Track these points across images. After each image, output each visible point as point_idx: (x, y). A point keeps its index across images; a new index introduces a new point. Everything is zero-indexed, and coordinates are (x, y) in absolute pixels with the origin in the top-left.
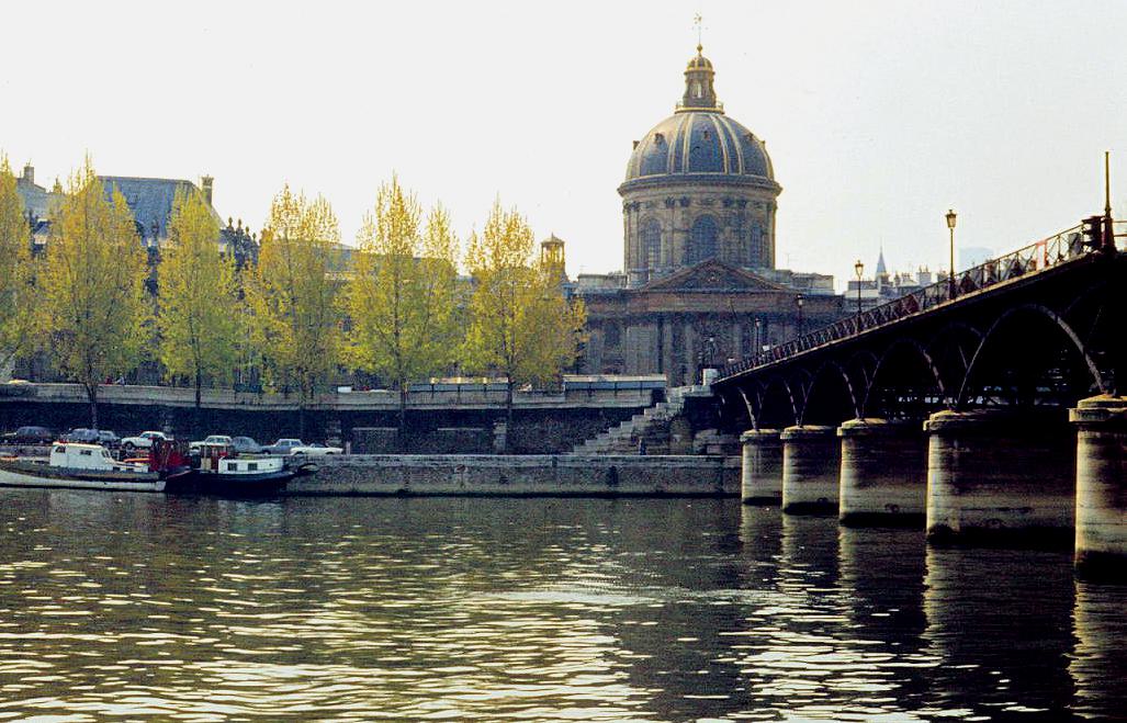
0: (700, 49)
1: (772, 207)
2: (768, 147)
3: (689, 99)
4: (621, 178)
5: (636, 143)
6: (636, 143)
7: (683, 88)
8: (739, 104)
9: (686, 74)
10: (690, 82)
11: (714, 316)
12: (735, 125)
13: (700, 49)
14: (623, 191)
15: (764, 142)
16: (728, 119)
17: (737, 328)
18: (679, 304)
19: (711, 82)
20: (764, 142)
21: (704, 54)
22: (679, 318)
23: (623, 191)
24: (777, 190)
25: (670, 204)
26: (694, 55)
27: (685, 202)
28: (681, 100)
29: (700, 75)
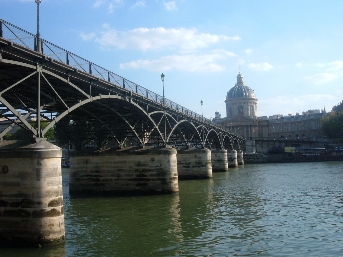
4: (225, 99)
5: (228, 92)
6: (228, 92)
7: (237, 80)
9: (237, 78)
10: (238, 79)
11: (240, 126)
13: (239, 72)
14: (225, 102)
15: (253, 90)
16: (245, 86)
17: (245, 128)
19: (242, 79)
20: (253, 90)
21: (240, 74)
22: (233, 127)
23: (225, 102)
25: (233, 104)
26: (239, 74)
27: (236, 104)
28: (236, 82)
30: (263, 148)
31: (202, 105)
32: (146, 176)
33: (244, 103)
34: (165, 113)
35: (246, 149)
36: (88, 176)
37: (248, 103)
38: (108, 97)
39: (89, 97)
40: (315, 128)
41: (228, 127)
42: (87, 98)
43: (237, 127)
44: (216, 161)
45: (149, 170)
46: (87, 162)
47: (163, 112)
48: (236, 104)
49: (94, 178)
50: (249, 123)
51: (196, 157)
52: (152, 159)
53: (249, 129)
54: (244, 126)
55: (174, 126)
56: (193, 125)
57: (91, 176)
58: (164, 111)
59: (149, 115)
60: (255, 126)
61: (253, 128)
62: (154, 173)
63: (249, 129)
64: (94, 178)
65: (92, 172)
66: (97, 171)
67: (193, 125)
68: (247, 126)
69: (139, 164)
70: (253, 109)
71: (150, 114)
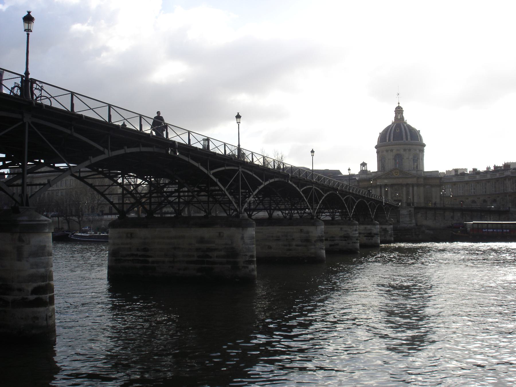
0: (399, 103)
1: (423, 151)
2: (421, 133)
3: (396, 118)
8: (411, 119)
10: (396, 113)
12: (409, 126)
13: (399, 103)
14: (376, 147)
18: (386, 181)
19: (402, 113)
21: (400, 105)
23: (376, 147)
24: (424, 145)
25: (387, 151)
27: (392, 150)
29: (399, 111)
30: (426, 219)
31: (313, 156)
32: (211, 257)
33: (405, 150)
34: (240, 170)
35: (401, 220)
36: (132, 255)
37: (410, 150)
38: (139, 151)
39: (106, 151)
40: (512, 191)
41: (378, 185)
42: (103, 153)
43: (392, 186)
44: (341, 237)
45: (215, 250)
46: (131, 236)
47: (237, 168)
48: (392, 150)
49: (140, 258)
50: (410, 181)
51: (301, 231)
52: (220, 233)
53: (411, 188)
54: (401, 185)
55: (257, 188)
56: (294, 185)
57: (136, 255)
58: (238, 167)
59: (210, 174)
60: (418, 185)
61: (415, 188)
62: (223, 253)
63: (411, 188)
64: (140, 258)
65: (138, 250)
66: (145, 250)
67: (294, 185)
68: (407, 185)
69: (202, 240)
70: (418, 158)
71: (212, 172)
